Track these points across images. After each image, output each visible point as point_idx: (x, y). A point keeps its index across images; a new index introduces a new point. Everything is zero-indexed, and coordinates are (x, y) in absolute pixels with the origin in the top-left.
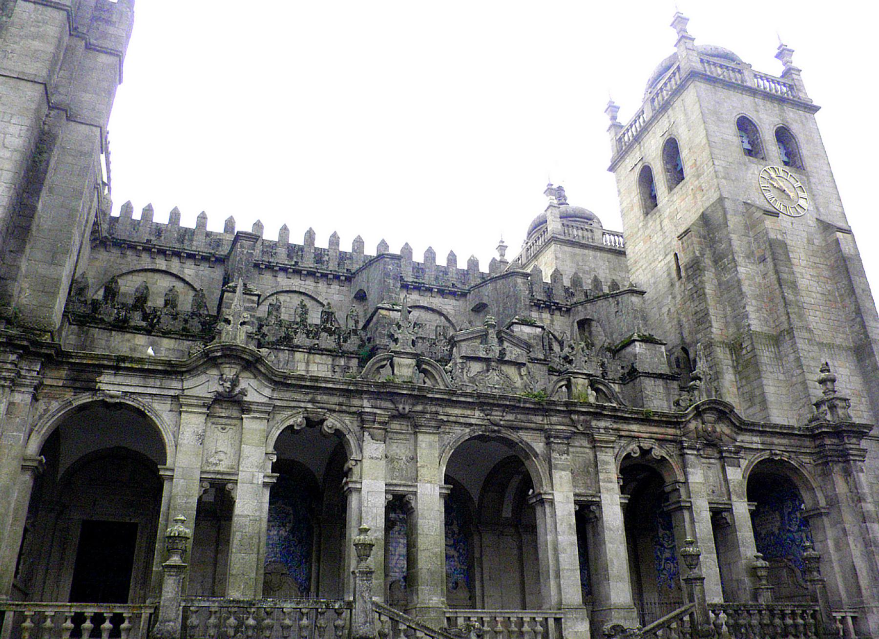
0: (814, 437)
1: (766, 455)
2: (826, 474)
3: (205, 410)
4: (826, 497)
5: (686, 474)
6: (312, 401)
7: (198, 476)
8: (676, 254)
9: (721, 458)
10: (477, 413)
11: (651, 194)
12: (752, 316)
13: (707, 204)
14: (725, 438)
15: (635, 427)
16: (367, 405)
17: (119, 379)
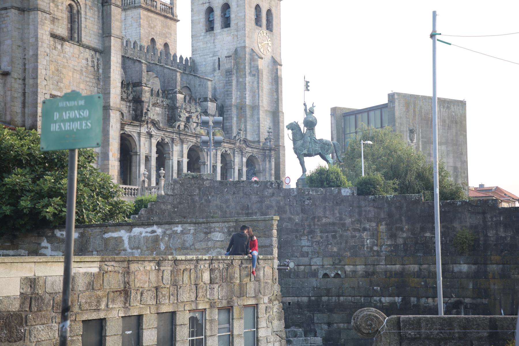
0: (263, 149)
1: (251, 154)
2: (264, 161)
3: (144, 136)
4: (262, 168)
5: (234, 159)
6: (164, 134)
7: (145, 155)
8: (219, 58)
9: (242, 155)
10: (195, 139)
11: (209, 19)
12: (247, 98)
13: (239, 45)
14: (244, 149)
15: (225, 144)
16: (174, 136)
17: (129, 127)
